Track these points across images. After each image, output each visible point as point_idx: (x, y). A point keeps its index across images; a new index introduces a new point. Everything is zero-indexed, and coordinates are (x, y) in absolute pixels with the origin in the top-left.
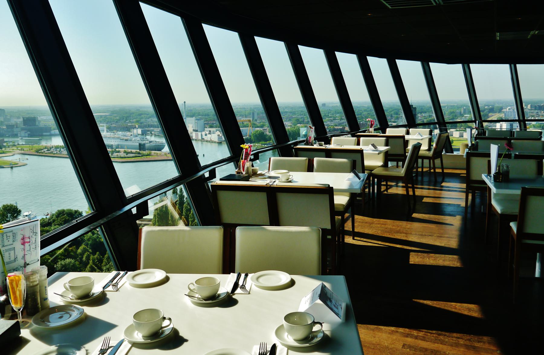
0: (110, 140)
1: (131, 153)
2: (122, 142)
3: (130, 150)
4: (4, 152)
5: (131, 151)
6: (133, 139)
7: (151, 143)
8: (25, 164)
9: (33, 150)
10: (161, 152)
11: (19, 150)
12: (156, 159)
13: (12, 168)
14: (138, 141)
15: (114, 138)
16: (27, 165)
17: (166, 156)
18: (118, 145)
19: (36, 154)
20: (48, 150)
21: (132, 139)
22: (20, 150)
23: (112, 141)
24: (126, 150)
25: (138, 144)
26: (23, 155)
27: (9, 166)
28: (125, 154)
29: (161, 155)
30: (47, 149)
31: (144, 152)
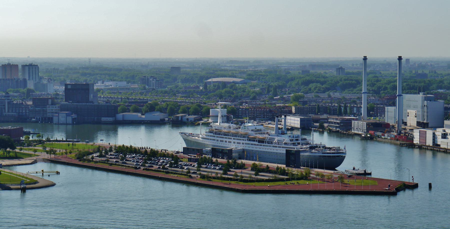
0: (228, 140)
1: (268, 170)
2: (252, 144)
3: (265, 164)
4: (19, 155)
5: (268, 167)
6: (276, 140)
7: (313, 151)
8: (50, 184)
9: (73, 155)
10: (332, 172)
11: (45, 153)
12: (318, 189)
13: (24, 190)
14: (286, 144)
15: (235, 135)
16: (53, 185)
17: (342, 182)
18: (243, 151)
19: (77, 162)
20: (101, 156)
21: (274, 139)
22: (47, 152)
23: (232, 141)
24: (257, 163)
25: (285, 152)
26: (52, 165)
27: (19, 187)
28: (254, 173)
29: (330, 180)
30: (98, 154)
31: (295, 171)
